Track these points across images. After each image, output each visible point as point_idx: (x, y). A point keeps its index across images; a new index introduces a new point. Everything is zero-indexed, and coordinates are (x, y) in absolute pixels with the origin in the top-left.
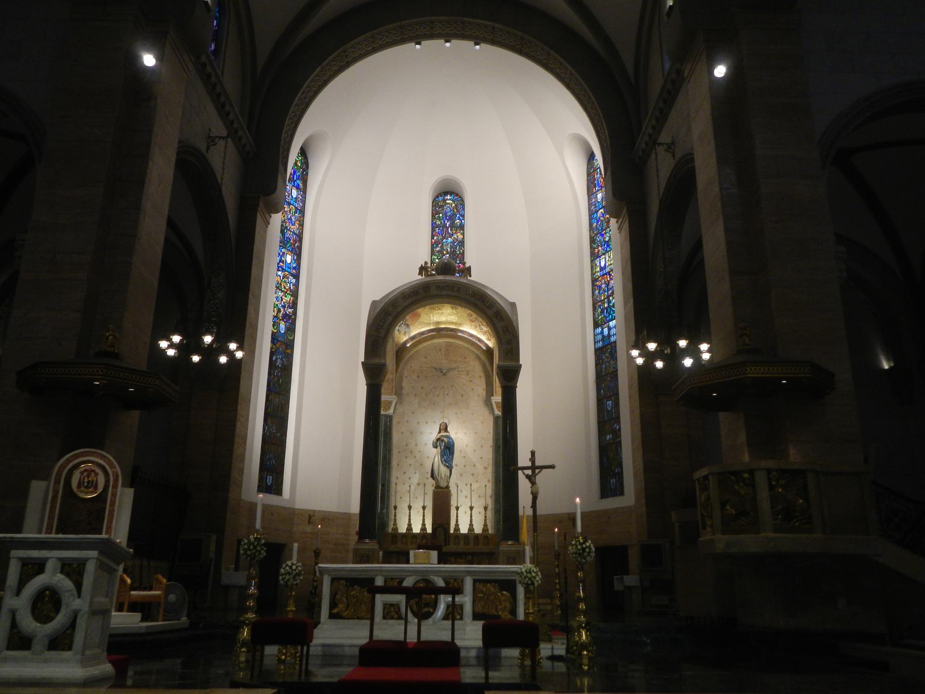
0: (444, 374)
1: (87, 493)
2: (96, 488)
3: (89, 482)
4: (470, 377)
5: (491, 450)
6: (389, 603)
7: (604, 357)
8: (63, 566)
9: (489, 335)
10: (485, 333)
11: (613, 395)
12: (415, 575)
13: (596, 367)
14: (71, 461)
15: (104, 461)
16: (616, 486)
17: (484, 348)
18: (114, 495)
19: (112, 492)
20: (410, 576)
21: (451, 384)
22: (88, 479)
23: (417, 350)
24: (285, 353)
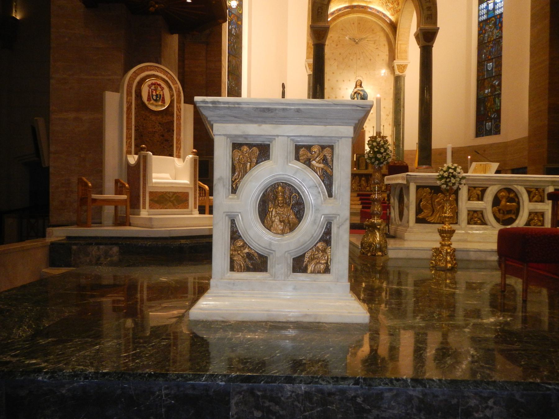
0: (357, 43)
1: (156, 106)
2: (163, 101)
3: (157, 95)
4: (377, 46)
5: (392, 101)
6: (474, 209)
7: (487, 28)
8: (298, 148)
9: (393, 11)
10: (390, 9)
11: (495, 58)
12: (499, 184)
13: (478, 38)
14: (138, 75)
15: (167, 76)
16: (491, 129)
17: (388, 22)
18: (179, 110)
19: (177, 106)
20: (495, 185)
21: (362, 51)
22: (156, 92)
23: (336, 24)
24: (237, 23)
